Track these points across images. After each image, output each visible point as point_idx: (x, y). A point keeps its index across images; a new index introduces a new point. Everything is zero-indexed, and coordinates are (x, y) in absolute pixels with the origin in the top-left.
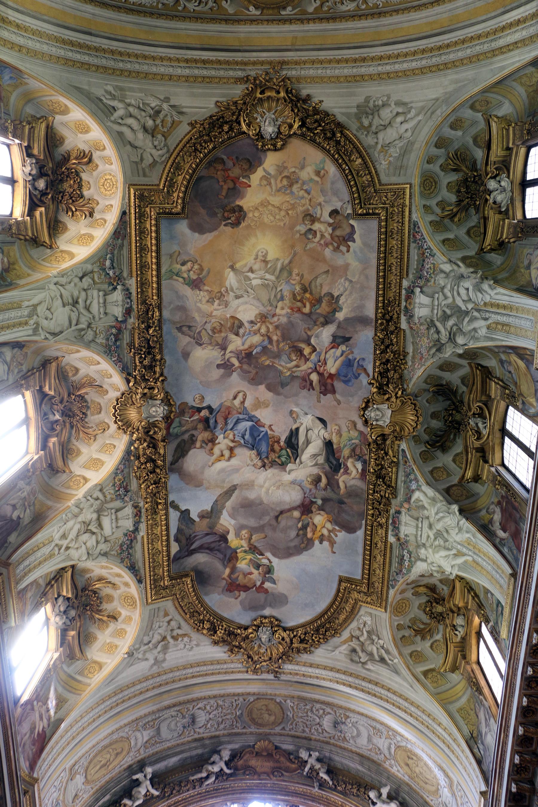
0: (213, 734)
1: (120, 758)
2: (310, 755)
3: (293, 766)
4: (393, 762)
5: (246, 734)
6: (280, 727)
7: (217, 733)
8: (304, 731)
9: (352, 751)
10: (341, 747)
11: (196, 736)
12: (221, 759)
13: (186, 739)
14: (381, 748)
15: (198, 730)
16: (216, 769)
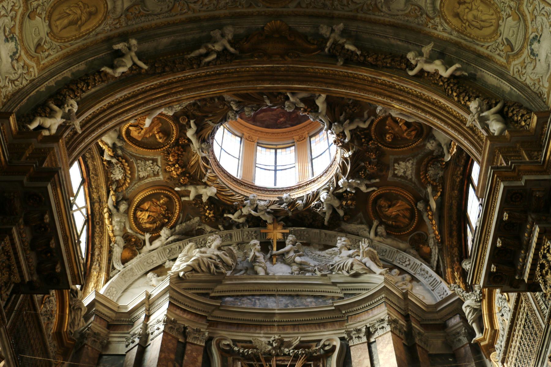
0: (212, 13)
1: (94, 22)
2: (333, 31)
3: (312, 47)
4: (437, 20)
5: (251, 15)
6: (294, 4)
7: (217, 13)
8: (324, 6)
9: (384, 24)
10: (370, 22)
11: (191, 14)
12: (223, 36)
13: (179, 17)
14: (423, 4)
15: (192, 5)
16: (217, 47)
